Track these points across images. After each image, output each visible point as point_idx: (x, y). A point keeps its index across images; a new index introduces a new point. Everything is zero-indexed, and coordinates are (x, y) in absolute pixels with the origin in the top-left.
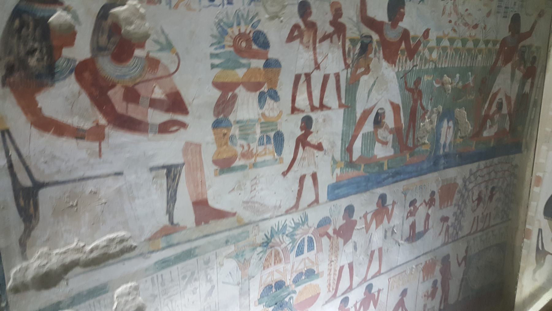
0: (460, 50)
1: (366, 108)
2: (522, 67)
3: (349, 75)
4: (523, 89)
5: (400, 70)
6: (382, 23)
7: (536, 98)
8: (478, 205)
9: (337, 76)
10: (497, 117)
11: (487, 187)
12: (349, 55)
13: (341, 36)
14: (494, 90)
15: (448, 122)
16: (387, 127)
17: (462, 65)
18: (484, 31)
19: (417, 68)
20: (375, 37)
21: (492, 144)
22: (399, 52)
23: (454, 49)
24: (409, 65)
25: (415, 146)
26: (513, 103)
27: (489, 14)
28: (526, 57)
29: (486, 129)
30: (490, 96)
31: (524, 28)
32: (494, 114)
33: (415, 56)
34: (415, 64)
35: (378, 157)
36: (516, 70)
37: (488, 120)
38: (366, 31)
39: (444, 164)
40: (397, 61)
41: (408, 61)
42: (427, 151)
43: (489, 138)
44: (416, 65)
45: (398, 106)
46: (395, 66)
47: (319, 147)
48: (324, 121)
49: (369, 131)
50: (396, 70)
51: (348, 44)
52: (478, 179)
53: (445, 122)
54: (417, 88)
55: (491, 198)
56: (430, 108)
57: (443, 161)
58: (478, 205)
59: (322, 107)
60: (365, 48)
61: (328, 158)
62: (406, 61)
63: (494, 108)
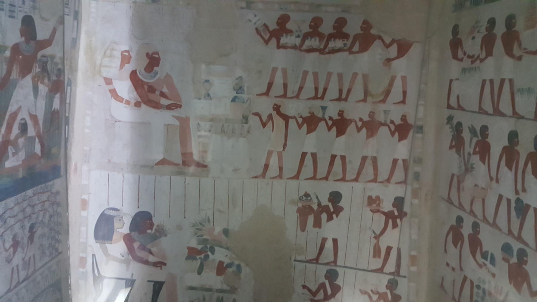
2: (46, 81)
8: (14, 252)
10: (21, 141)
11: (23, 227)
14: (12, 108)
21: (21, 175)
26: (41, 122)
28: (49, 67)
29: (7, 158)
30: (7, 117)
31: (42, 34)
32: (17, 138)
36: (39, 83)
37: (10, 147)
43: (15, 169)
52: (8, 221)
55: (31, 238)
58: (14, 252)
63: (16, 130)
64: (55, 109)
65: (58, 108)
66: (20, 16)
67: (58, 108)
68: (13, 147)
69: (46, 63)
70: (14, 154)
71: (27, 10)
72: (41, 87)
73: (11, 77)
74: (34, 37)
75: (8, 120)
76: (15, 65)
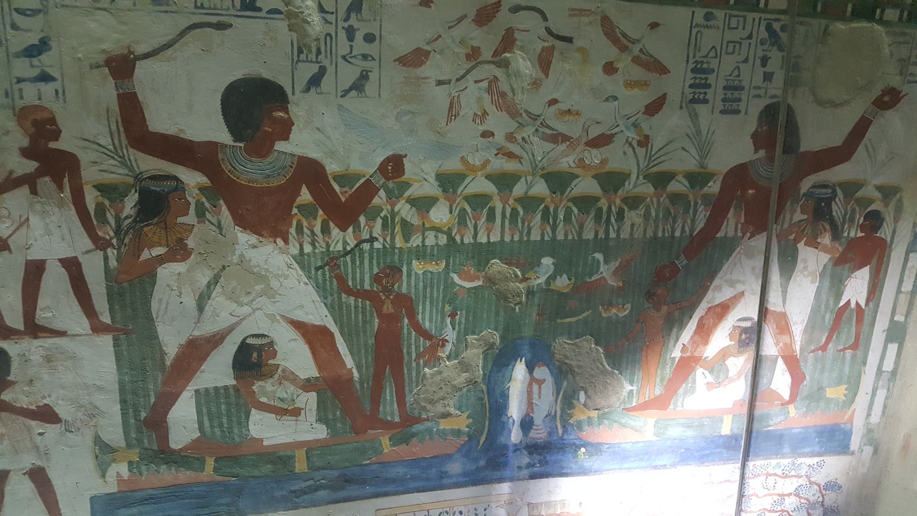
0: (543, 200)
1: (197, 333)
2: (826, 240)
3: (113, 263)
5: (308, 249)
6: (213, 147)
7: (899, 318)
9: (72, 266)
12: (104, 221)
13: (66, 180)
15: (530, 368)
16: (289, 377)
17: (560, 236)
18: (641, 152)
19: (377, 245)
20: (193, 179)
22: (295, 211)
23: (519, 200)
24: (341, 239)
25: (408, 420)
27: (654, 108)
28: (837, 209)
32: (724, 354)
33: (362, 219)
34: (365, 235)
35: (265, 443)
38: (149, 164)
39: (529, 465)
40: (293, 231)
41: (335, 231)
42: (458, 433)
44: (372, 240)
45: (323, 331)
46: (286, 241)
47: (47, 415)
48: (48, 359)
49: (220, 384)
50: (295, 251)
51: (91, 198)
53: (520, 370)
54: (387, 291)
56: (450, 334)
57: (526, 460)
59: (34, 329)
60: (157, 203)
61: (84, 440)
62: (325, 230)
64: (849, 302)
65: (863, 303)
66: (756, 107)
67: (863, 303)
68: (711, 372)
70: (710, 386)
71: (779, 92)
74: (791, 147)
76: (732, 210)
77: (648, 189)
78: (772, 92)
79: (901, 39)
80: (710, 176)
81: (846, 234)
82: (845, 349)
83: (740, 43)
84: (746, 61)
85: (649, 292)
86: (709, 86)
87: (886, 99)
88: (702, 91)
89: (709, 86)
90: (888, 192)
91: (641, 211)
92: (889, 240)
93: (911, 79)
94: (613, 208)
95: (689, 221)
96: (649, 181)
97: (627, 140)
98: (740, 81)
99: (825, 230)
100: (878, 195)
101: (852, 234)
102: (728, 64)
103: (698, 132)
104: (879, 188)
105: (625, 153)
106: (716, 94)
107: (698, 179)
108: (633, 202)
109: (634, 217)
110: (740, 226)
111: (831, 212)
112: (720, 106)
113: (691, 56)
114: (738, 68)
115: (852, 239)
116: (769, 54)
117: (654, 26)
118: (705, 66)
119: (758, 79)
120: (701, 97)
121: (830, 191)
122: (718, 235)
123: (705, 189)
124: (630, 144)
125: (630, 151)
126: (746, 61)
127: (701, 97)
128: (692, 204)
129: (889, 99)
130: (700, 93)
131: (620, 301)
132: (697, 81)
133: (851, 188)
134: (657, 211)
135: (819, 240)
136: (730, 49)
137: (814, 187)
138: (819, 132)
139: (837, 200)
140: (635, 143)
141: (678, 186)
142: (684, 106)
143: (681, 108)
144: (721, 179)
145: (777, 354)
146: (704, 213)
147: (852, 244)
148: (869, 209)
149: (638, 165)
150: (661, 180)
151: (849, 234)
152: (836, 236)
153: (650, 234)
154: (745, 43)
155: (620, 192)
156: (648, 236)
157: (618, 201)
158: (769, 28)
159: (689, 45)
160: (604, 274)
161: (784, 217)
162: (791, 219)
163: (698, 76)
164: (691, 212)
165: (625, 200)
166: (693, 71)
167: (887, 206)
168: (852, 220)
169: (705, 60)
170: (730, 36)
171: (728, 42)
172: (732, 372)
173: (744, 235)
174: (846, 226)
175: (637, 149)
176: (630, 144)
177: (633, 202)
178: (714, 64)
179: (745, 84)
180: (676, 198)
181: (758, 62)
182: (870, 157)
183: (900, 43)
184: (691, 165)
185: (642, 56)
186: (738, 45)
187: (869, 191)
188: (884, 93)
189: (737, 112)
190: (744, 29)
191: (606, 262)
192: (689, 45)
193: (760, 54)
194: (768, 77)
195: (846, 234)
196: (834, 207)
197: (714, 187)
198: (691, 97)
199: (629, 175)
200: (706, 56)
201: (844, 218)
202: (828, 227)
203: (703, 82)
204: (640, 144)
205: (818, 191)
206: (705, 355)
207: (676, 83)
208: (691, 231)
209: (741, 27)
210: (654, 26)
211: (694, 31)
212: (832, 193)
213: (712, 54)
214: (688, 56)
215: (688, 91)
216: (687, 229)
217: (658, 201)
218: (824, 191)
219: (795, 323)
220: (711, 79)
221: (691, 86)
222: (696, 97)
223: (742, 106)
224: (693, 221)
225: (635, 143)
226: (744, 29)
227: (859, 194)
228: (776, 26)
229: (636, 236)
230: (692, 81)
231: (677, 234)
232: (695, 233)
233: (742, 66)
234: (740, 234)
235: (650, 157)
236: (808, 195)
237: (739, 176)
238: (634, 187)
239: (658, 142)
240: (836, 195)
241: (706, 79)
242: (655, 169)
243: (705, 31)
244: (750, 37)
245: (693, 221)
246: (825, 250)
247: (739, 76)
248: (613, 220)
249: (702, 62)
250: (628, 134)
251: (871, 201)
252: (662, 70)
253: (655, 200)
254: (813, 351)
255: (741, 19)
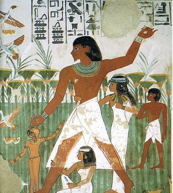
2: (128, 104)
4: (143, 136)
14: (67, 132)
18: (15, 61)
26: (122, 155)
30: (58, 143)
32: (75, 168)
36: (114, 108)
37: (63, 177)
65: (160, 140)
67: (160, 140)
68: (70, 178)
69: (125, 84)
72: (117, 111)
73: (64, 101)
75: (60, 146)
76: (68, 89)
77: (21, 79)
78: (77, 33)
79: (146, 5)
80: (52, 73)
81: (139, 102)
82: (154, 168)
83: (58, 12)
84: (62, 20)
85: (29, 131)
86: (45, 31)
87: (145, 32)
88: (42, 34)
89: (45, 31)
90: (159, 78)
91: (19, 89)
92: (167, 104)
93: (157, 23)
94: (5, 88)
95: (45, 95)
96: (22, 75)
97: (7, 56)
98: (61, 28)
99: (127, 100)
100: (153, 80)
101: (143, 102)
102: (53, 22)
103: (43, 52)
104: (154, 77)
105: (7, 62)
106: (49, 34)
107: (48, 73)
108: (15, 85)
109: (16, 92)
110: (73, 97)
111: (128, 90)
112: (52, 40)
113: (34, 19)
114: (58, 22)
115: (144, 104)
116: (73, 16)
117: (14, 7)
118: (41, 23)
119: (70, 27)
120: (42, 36)
121: (124, 79)
122: (62, 102)
123: (52, 79)
124: (9, 58)
125: (9, 61)
126: (62, 20)
127: (42, 36)
128: (46, 86)
129: (147, 33)
130: (41, 35)
131: (14, 136)
132: (39, 29)
133: (137, 77)
134: (27, 89)
135: (124, 105)
136: (53, 15)
137: (114, 77)
138: (109, 50)
139: (130, 83)
140: (11, 57)
141: (36, 77)
142: (34, 40)
143: (32, 41)
144: (59, 73)
145: (112, 169)
146: (53, 91)
147: (144, 107)
148: (150, 88)
149: (15, 67)
150: (28, 74)
151: (141, 101)
152: (134, 102)
153: (25, 100)
154: (60, 12)
155: (7, 80)
156: (25, 102)
157: (7, 85)
158: (71, 4)
159: (32, 14)
160: (4, 121)
161: (100, 92)
162: (105, 94)
163: (38, 27)
164: (46, 90)
165: (10, 84)
166: (35, 25)
167: (160, 86)
168: (141, 94)
169: (41, 20)
170: (51, 9)
171: (51, 12)
172: (83, 178)
173: (77, 102)
174: (139, 97)
175: (13, 60)
176: (9, 58)
177: (15, 85)
178: (46, 22)
179: (63, 29)
180: (35, 83)
181: (68, 20)
182: (143, 61)
183: (145, 7)
184: (42, 67)
185: (9, 20)
186: (56, 13)
187: (147, 79)
188: (143, 30)
189: (62, 42)
190: (58, 6)
191: (4, 115)
192: (32, 14)
193: (68, 16)
194: (75, 26)
195: (139, 102)
196: (129, 88)
197: (56, 78)
198: (36, 36)
199: (11, 72)
200: (41, 19)
201: (136, 93)
202: (127, 98)
203: (42, 30)
204: (14, 57)
205: (117, 79)
206: (65, 167)
207: (28, 31)
208: (48, 99)
209: (57, 5)
210: (14, 7)
211: (34, 8)
212: (126, 80)
213: (44, 17)
214: (32, 19)
215: (35, 34)
216: (45, 99)
217: (27, 85)
218: (121, 79)
219: (120, 151)
220: (46, 28)
221: (36, 32)
222: (39, 36)
223: (64, 40)
224: (48, 94)
225: (11, 57)
226: (58, 6)
227: (143, 80)
228: (75, 4)
229: (18, 102)
230: (36, 30)
231: (40, 101)
232: (49, 102)
233: (60, 22)
234: (74, 101)
235: (20, 64)
236: (112, 81)
237: (67, 72)
238: (14, 78)
239: (23, 57)
240: (128, 81)
241: (43, 28)
242: (23, 70)
243: (39, 8)
244: (62, 9)
245: (48, 94)
246: (129, 110)
247: (59, 26)
248: (5, 94)
249: (40, 21)
250: (8, 53)
251: (151, 84)
252: (20, 25)
253: (26, 84)
254: (134, 168)
255: (56, 2)
